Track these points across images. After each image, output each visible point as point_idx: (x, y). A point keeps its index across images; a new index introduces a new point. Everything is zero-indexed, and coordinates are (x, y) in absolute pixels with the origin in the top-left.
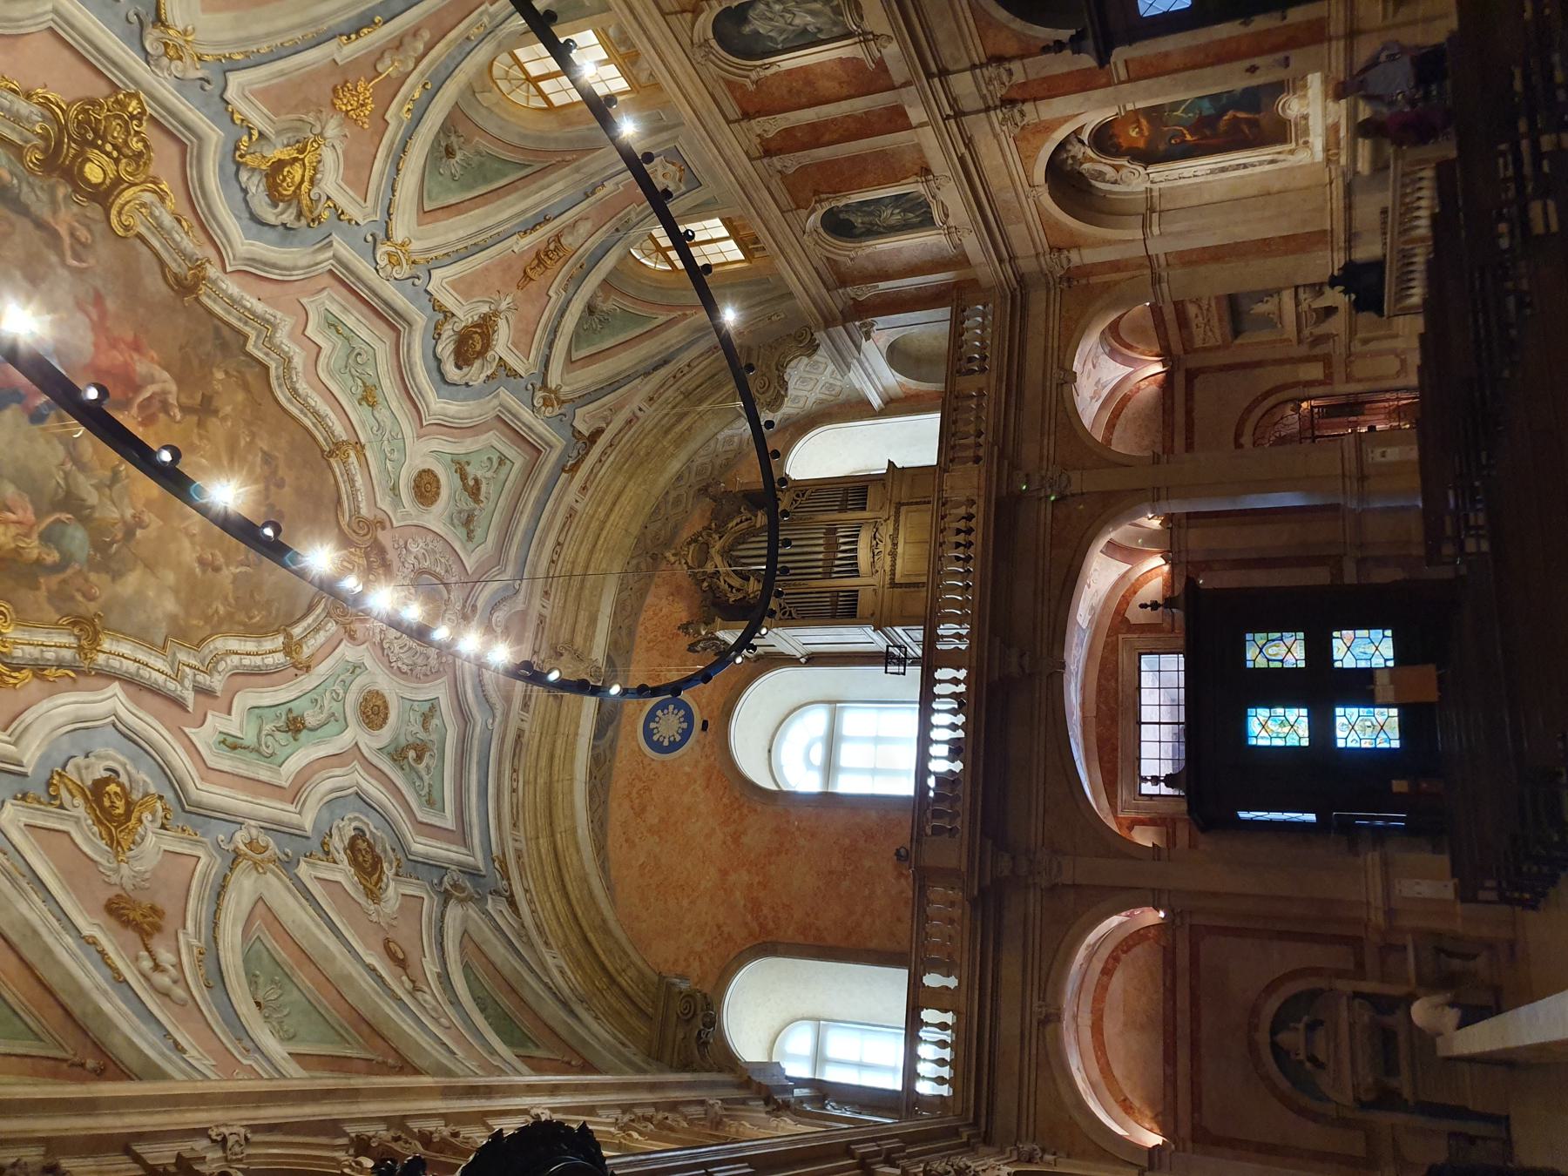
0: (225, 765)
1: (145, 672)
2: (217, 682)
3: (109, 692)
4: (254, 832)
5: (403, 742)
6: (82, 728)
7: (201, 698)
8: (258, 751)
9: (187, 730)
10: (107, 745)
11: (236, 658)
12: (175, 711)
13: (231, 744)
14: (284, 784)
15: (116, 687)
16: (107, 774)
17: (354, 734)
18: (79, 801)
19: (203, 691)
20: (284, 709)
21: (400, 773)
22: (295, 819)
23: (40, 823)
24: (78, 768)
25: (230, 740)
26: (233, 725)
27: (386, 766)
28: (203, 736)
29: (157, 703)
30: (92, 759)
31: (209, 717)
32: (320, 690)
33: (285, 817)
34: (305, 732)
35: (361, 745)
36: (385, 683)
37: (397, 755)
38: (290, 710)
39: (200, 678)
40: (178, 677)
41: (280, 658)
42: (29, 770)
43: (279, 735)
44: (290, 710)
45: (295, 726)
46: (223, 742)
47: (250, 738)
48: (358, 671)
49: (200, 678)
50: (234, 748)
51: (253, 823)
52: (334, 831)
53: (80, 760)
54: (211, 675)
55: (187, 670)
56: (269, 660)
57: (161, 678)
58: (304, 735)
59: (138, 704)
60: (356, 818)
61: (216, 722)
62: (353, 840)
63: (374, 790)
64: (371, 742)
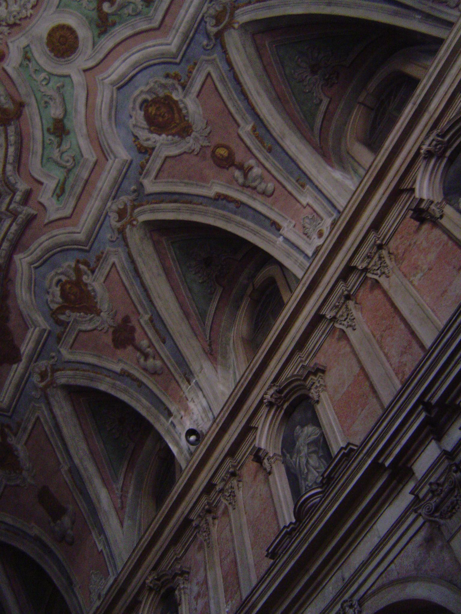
0: (72, 203)
1: (10, 236)
2: (22, 186)
3: (18, 262)
4: (114, 207)
5: (94, 14)
6: (35, 285)
7: (30, 202)
8: (69, 171)
9: (46, 221)
10: (44, 277)
11: (9, 167)
12: (35, 223)
13: (60, 191)
14: (94, 159)
15: (17, 257)
16: (58, 289)
17: (74, 68)
18: (68, 312)
19: (28, 196)
20: (46, 134)
21: (117, 28)
22: (117, 164)
23: (71, 341)
24: (53, 301)
25: (58, 191)
26: (51, 185)
27: (107, 42)
28: (55, 209)
29: (29, 233)
30: (51, 291)
31: (42, 200)
32: (39, 96)
33: (114, 173)
34: (65, 121)
35: (86, 67)
36: (44, 25)
37: (103, 25)
38: (48, 130)
39: (18, 197)
40: (15, 215)
41: (11, 129)
42: (49, 328)
43: (64, 147)
44: (48, 130)
45: (59, 129)
46: (59, 196)
47: (59, 174)
48: (29, 55)
49: (18, 197)
50: (63, 190)
51: (109, 204)
52: (135, 131)
53: (49, 298)
54: (17, 190)
55: (12, 207)
56: (12, 138)
57: (14, 227)
58: (68, 125)
59: (27, 247)
60: (134, 102)
61: (46, 197)
62: (148, 118)
63: (119, 68)
64: (84, 58)
